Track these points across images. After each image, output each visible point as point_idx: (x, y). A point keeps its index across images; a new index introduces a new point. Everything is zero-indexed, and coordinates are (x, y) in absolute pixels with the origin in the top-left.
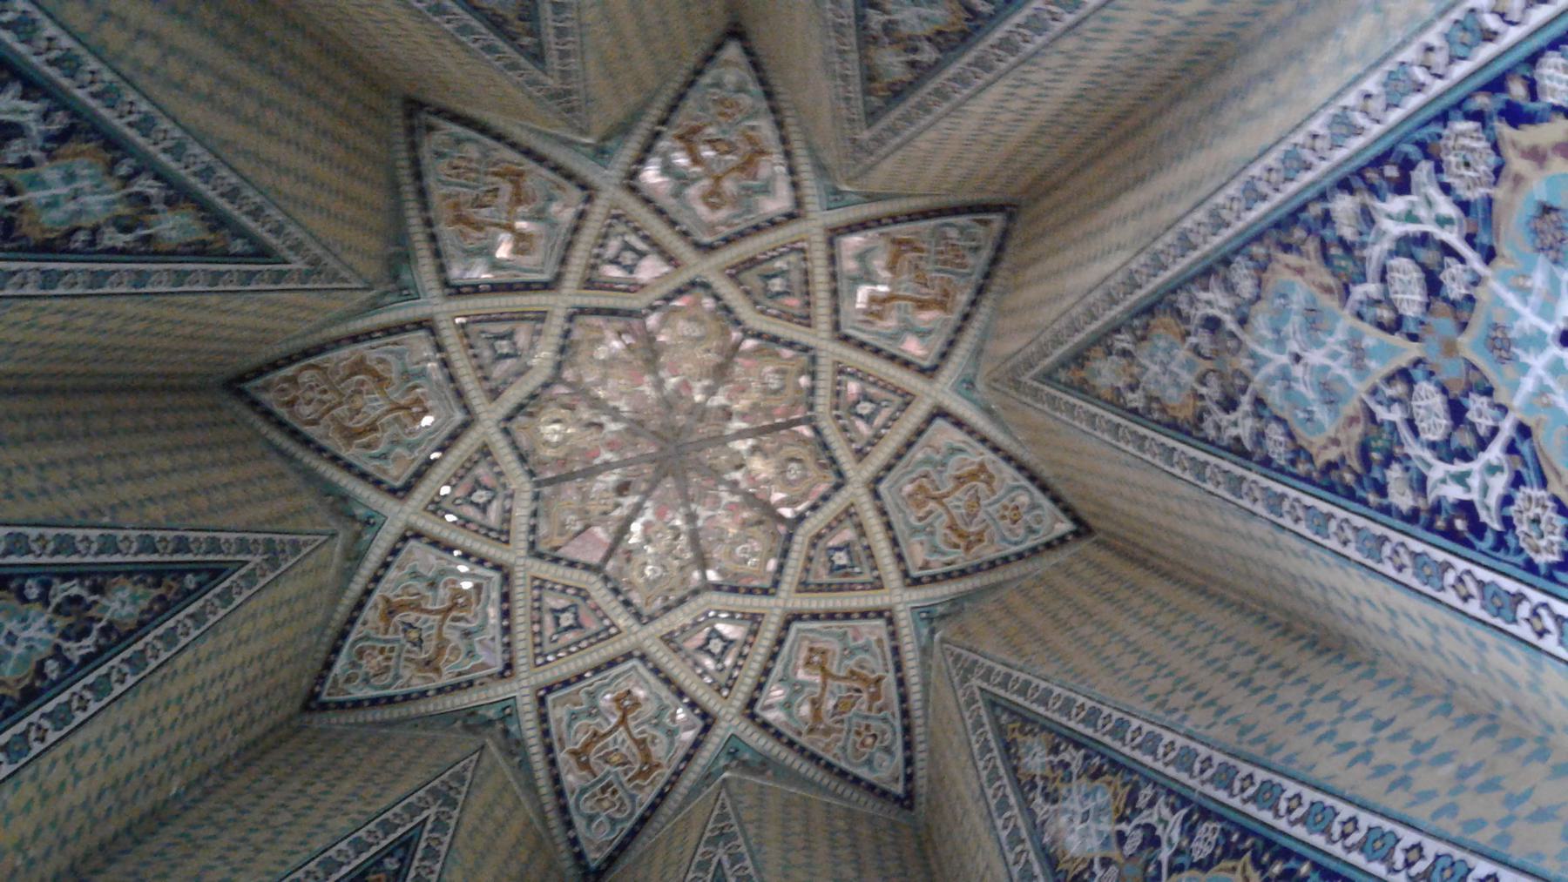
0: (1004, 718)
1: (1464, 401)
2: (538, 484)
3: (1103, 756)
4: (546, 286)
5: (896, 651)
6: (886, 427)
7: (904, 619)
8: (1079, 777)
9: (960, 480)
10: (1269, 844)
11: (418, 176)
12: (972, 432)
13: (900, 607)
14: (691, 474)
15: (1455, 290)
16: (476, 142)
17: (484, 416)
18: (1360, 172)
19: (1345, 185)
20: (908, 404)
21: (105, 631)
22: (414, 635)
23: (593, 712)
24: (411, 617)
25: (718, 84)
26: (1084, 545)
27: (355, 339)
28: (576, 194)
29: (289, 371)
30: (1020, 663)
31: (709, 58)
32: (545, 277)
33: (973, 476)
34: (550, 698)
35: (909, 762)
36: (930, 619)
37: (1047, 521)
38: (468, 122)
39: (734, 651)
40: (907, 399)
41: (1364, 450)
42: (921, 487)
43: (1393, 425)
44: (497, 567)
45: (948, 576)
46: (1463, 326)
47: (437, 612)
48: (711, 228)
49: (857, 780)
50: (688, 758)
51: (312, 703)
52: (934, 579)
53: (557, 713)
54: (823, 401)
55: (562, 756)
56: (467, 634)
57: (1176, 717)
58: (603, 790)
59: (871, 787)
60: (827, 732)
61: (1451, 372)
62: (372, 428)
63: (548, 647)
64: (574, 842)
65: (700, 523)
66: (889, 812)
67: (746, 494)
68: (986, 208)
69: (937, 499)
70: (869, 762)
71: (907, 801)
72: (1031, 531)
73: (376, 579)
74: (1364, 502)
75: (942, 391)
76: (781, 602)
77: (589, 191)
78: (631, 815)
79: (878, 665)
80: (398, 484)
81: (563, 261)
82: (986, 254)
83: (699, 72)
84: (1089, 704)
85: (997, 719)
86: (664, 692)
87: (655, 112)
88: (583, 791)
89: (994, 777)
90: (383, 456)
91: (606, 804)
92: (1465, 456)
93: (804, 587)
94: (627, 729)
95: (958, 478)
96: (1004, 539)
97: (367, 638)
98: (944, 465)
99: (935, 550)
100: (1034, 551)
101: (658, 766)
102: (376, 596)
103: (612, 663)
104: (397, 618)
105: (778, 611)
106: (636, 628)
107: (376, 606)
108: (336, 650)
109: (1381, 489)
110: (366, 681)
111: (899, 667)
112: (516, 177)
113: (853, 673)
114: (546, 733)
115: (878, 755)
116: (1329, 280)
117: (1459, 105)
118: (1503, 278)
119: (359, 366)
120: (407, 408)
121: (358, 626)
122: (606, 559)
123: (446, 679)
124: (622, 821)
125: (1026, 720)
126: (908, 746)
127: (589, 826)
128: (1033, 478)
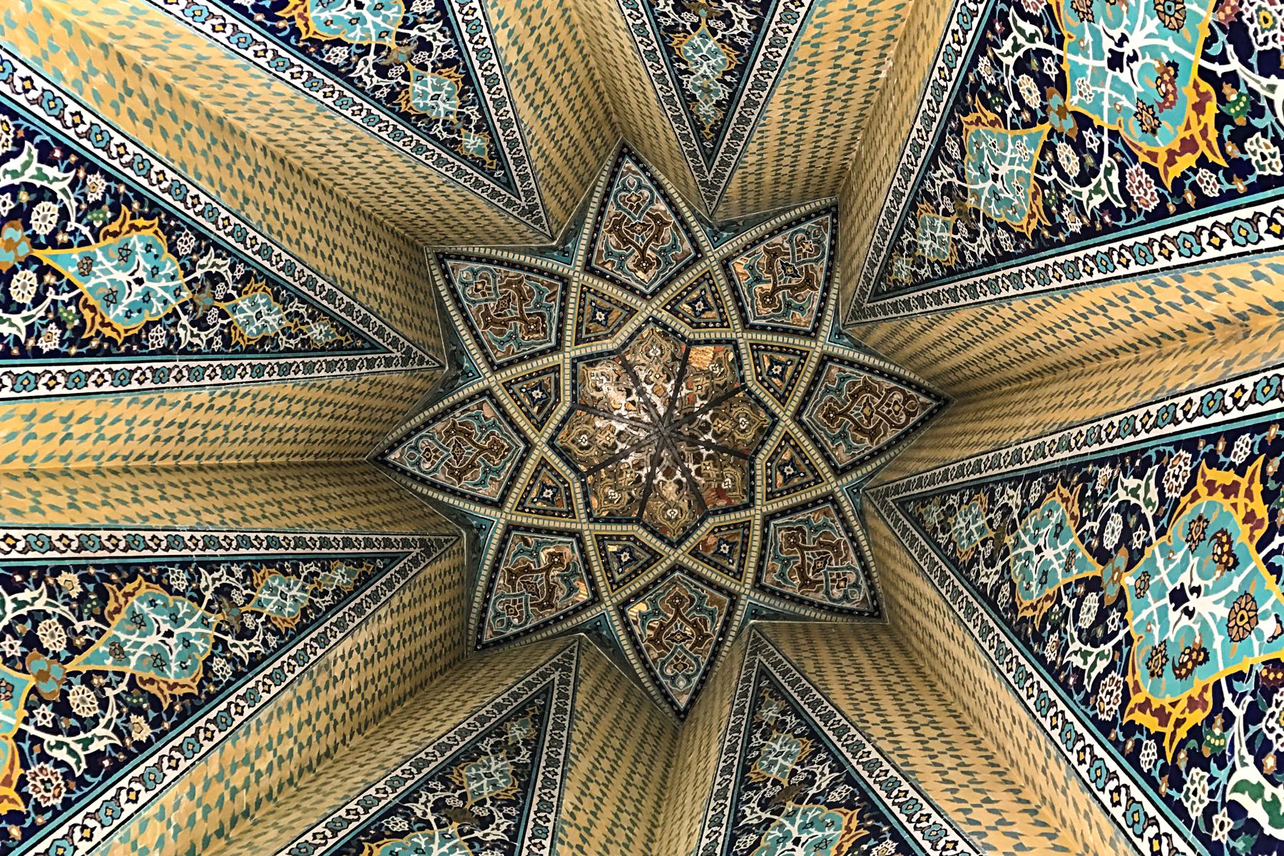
0: (359, 343)
1: (25, 650)
3: (264, 352)
5: (481, 346)
6: (532, 486)
7: (485, 369)
8: (277, 334)
9: (473, 465)
10: (108, 353)
11: (865, 568)
12: (472, 499)
13: (488, 375)
15: (47, 710)
16: (834, 601)
17: (789, 422)
18: (131, 756)
19: (141, 746)
20: (520, 503)
21: (902, 251)
24: (794, 283)
25: (688, 678)
26: (373, 452)
27: (880, 451)
28: (767, 580)
29: (912, 421)
30: (364, 378)
31: (697, 693)
32: (772, 523)
33: (464, 472)
35: (449, 282)
36: (464, 373)
38: (841, 611)
39: (587, 316)
40: (521, 507)
41: (103, 597)
42: (497, 455)
43: (80, 619)
44: (753, 327)
45: (463, 403)
46: (34, 690)
47: (780, 289)
48: (673, 582)
49: (479, 260)
51: (833, 210)
52: (472, 398)
53: (687, 245)
54: (577, 489)
55: (673, 220)
56: (758, 280)
57: (218, 392)
58: (639, 206)
59: (468, 258)
60: (509, 284)
61: (38, 663)
62: (854, 397)
63: (705, 285)
64: (645, 170)
66: (448, 248)
68: (496, 643)
69: (483, 449)
70: (475, 273)
71: (441, 258)
73: (824, 299)
74: (96, 567)
75: (499, 519)
78: (616, 196)
79: (487, 335)
81: (765, 536)
82: (491, 613)
84: (292, 375)
85: (365, 341)
86: (623, 277)
88: (651, 202)
89: (349, 309)
90: (842, 380)
91: (634, 198)
92: (21, 619)
93: (556, 369)
94: (638, 248)
95: (474, 466)
96: (432, 438)
97: (817, 261)
99: (477, 417)
100: (409, 436)
101: (610, 231)
102: (820, 289)
107: (818, 284)
108: (832, 247)
109: (85, 579)
110: (807, 233)
111: (476, 337)
112: (805, 583)
113: (506, 326)
114: (688, 231)
116: (148, 687)
117: (57, 814)
118: (10, 726)
119: (872, 435)
120: (838, 415)
121: (824, 266)
122: (688, 351)
123: (760, 248)
124: (620, 191)
125: (340, 348)
126: (453, 291)
127: (639, 182)
128: (423, 481)
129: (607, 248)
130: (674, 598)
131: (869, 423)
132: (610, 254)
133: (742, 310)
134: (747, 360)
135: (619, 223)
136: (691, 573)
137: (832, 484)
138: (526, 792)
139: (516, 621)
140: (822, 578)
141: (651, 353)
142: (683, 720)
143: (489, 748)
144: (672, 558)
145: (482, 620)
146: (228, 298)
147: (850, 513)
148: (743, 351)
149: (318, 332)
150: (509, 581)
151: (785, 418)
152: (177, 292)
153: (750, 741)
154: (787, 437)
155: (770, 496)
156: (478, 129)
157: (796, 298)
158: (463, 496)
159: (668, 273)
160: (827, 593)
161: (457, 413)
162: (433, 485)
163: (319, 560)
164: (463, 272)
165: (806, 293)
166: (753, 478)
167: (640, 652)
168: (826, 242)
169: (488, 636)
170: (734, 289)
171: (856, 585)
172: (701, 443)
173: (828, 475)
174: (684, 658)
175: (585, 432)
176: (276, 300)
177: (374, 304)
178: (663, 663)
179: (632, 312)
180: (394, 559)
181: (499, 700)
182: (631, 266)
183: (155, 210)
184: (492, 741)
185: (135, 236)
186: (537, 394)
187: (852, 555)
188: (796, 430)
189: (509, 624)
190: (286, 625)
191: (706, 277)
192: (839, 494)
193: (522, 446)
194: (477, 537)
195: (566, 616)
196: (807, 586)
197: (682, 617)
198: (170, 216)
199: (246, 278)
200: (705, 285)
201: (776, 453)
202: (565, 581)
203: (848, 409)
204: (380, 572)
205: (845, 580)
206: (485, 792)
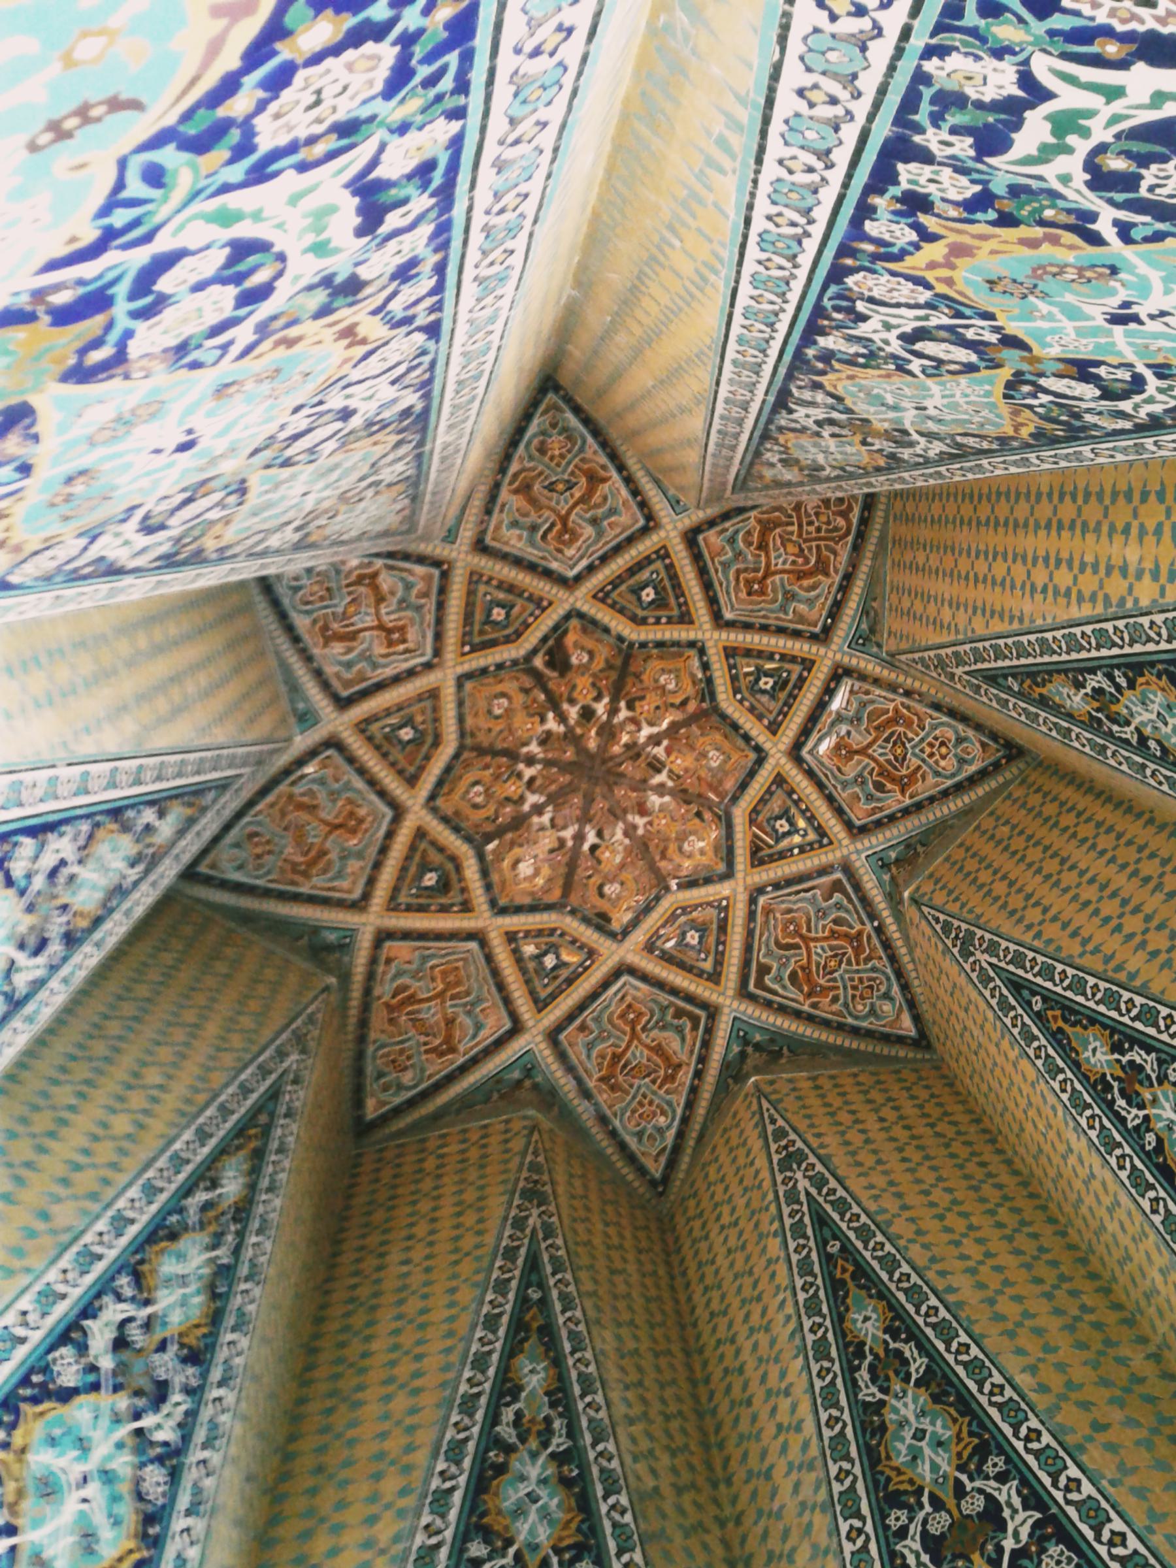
2: (631, 645)
4: (797, 746)
5: (325, 902)
9: (450, 1022)
14: (568, 778)
16: (953, 775)
17: (716, 635)
20: (536, 1001)
22: (561, 487)
23: (403, 604)
24: (577, 495)
25: (887, 996)
27: (848, 577)
31: (912, 1004)
32: (804, 753)
33: (448, 1039)
34: (436, 573)
37: (383, 1097)
38: (973, 781)
40: (541, 1005)
44: (578, 579)
45: (370, 976)
48: (768, 911)
50: (318, 673)
52: (373, 961)
53: (420, 570)
56: (534, 528)
60: (283, 814)
62: (763, 546)
65: (521, 766)
67: (528, 816)
68: (672, 1164)
69: (441, 995)
72: (380, 1075)
73: (629, 480)
75: (532, 1041)
76: (417, 808)
77: (857, 831)
80: (700, 538)
81: (810, 774)
82: (632, 1143)
83: (905, 987)
86: (388, 672)
87: (892, 929)
90: (732, 541)
93: (420, 833)
97: (581, 450)
98: (469, 1013)
99: (399, 974)
100: (359, 1072)
103: (438, 636)
104: (583, 481)
105: (409, 803)
106: (460, 670)
107: (604, 467)
108: (587, 421)
110: (543, 433)
115: (242, 854)
119: (822, 568)
121: (596, 446)
123: (504, 494)
125: (258, 1155)
128: (425, 1095)
129: (340, 663)
130: (785, 928)
131: (807, 561)
132: (349, 665)
133: (548, 574)
134: (604, 615)
135: (325, 628)
136: (777, 886)
137: (827, 657)
138: (974, 1416)
139: (662, 1121)
140: (915, 762)
141: (498, 711)
142: (929, 1047)
143: (874, 1390)
144: (741, 889)
145: (631, 1158)
146: (148, 1325)
147: (878, 669)
148: (593, 612)
149: (231, 1187)
150: (613, 1088)
151: (708, 635)
152: (117, 1420)
153: (1123, 1121)
154: (730, 652)
155: (774, 728)
156: (161, 814)
157: (597, 506)
158: (475, 1061)
159: (430, 618)
160: (937, 774)
161: (377, 992)
162: (438, 1087)
163: (502, 1395)
164: (228, 867)
165: (605, 488)
166: (735, 727)
167: (810, 1019)
168: (573, 420)
169: (656, 1170)
170: (518, 562)
171: (960, 740)
172: (646, 744)
173: (814, 649)
174: (861, 980)
175: (517, 862)
176: (173, 1236)
177: (228, 1059)
178: (846, 1005)
179: (433, 694)
180: (533, 1264)
181: (802, 1296)
182: (384, 651)
183: (12, 1401)
184: (863, 1375)
185: (31, 1457)
186: (430, 879)
187: (921, 709)
188: (732, 636)
189: (661, 1131)
190: (574, 1526)
191: (475, 578)
192: (846, 660)
193: (473, 945)
194: (536, 1087)
195: (702, 1060)
196: (908, 785)
197: (816, 940)
198: (25, 1381)
199: (138, 1278)
200: (482, 588)
201: (734, 679)
202: (664, 1028)
203: (768, 565)
204: (544, 1302)
205: (943, 744)
206: (945, 1467)
